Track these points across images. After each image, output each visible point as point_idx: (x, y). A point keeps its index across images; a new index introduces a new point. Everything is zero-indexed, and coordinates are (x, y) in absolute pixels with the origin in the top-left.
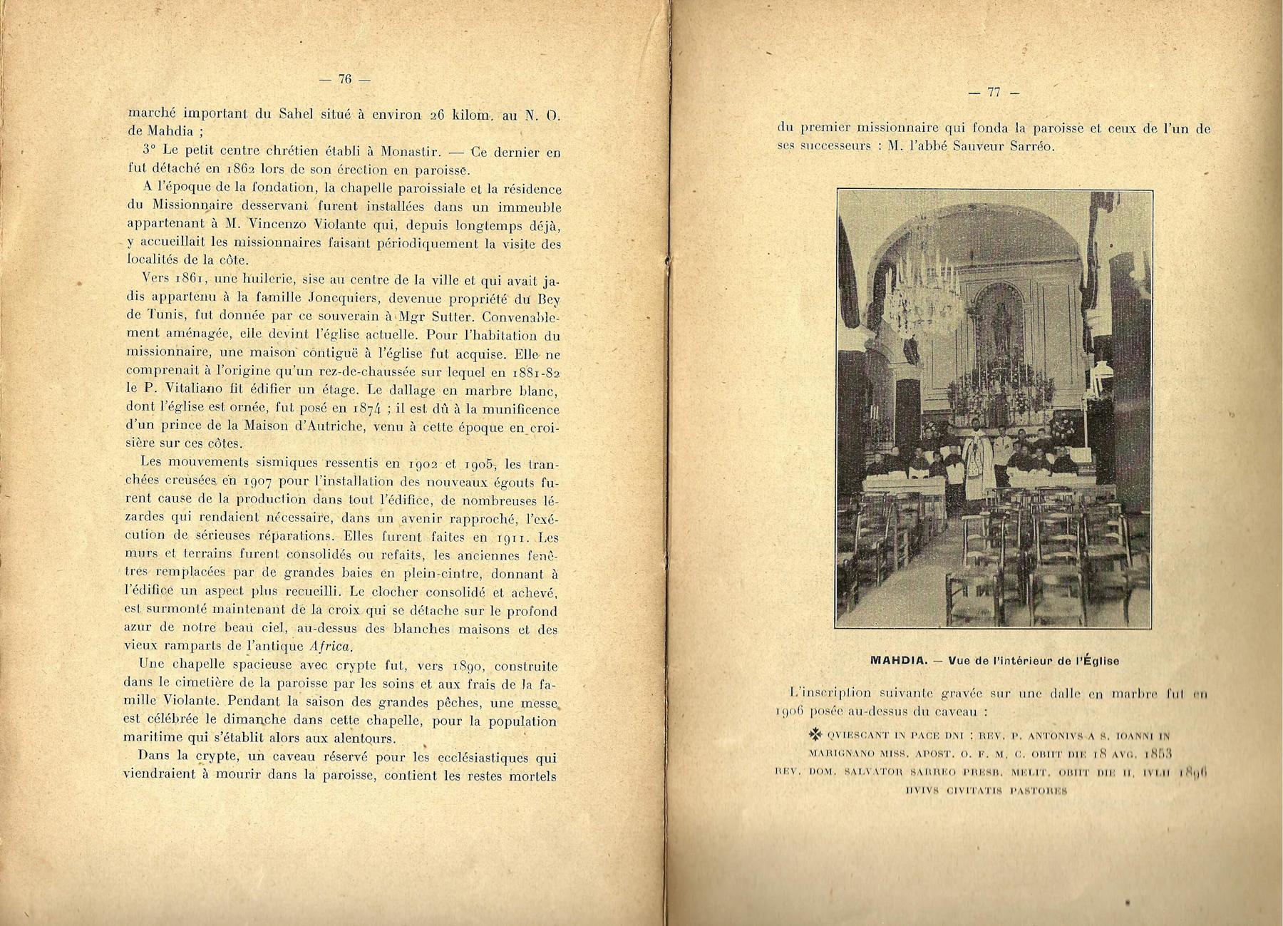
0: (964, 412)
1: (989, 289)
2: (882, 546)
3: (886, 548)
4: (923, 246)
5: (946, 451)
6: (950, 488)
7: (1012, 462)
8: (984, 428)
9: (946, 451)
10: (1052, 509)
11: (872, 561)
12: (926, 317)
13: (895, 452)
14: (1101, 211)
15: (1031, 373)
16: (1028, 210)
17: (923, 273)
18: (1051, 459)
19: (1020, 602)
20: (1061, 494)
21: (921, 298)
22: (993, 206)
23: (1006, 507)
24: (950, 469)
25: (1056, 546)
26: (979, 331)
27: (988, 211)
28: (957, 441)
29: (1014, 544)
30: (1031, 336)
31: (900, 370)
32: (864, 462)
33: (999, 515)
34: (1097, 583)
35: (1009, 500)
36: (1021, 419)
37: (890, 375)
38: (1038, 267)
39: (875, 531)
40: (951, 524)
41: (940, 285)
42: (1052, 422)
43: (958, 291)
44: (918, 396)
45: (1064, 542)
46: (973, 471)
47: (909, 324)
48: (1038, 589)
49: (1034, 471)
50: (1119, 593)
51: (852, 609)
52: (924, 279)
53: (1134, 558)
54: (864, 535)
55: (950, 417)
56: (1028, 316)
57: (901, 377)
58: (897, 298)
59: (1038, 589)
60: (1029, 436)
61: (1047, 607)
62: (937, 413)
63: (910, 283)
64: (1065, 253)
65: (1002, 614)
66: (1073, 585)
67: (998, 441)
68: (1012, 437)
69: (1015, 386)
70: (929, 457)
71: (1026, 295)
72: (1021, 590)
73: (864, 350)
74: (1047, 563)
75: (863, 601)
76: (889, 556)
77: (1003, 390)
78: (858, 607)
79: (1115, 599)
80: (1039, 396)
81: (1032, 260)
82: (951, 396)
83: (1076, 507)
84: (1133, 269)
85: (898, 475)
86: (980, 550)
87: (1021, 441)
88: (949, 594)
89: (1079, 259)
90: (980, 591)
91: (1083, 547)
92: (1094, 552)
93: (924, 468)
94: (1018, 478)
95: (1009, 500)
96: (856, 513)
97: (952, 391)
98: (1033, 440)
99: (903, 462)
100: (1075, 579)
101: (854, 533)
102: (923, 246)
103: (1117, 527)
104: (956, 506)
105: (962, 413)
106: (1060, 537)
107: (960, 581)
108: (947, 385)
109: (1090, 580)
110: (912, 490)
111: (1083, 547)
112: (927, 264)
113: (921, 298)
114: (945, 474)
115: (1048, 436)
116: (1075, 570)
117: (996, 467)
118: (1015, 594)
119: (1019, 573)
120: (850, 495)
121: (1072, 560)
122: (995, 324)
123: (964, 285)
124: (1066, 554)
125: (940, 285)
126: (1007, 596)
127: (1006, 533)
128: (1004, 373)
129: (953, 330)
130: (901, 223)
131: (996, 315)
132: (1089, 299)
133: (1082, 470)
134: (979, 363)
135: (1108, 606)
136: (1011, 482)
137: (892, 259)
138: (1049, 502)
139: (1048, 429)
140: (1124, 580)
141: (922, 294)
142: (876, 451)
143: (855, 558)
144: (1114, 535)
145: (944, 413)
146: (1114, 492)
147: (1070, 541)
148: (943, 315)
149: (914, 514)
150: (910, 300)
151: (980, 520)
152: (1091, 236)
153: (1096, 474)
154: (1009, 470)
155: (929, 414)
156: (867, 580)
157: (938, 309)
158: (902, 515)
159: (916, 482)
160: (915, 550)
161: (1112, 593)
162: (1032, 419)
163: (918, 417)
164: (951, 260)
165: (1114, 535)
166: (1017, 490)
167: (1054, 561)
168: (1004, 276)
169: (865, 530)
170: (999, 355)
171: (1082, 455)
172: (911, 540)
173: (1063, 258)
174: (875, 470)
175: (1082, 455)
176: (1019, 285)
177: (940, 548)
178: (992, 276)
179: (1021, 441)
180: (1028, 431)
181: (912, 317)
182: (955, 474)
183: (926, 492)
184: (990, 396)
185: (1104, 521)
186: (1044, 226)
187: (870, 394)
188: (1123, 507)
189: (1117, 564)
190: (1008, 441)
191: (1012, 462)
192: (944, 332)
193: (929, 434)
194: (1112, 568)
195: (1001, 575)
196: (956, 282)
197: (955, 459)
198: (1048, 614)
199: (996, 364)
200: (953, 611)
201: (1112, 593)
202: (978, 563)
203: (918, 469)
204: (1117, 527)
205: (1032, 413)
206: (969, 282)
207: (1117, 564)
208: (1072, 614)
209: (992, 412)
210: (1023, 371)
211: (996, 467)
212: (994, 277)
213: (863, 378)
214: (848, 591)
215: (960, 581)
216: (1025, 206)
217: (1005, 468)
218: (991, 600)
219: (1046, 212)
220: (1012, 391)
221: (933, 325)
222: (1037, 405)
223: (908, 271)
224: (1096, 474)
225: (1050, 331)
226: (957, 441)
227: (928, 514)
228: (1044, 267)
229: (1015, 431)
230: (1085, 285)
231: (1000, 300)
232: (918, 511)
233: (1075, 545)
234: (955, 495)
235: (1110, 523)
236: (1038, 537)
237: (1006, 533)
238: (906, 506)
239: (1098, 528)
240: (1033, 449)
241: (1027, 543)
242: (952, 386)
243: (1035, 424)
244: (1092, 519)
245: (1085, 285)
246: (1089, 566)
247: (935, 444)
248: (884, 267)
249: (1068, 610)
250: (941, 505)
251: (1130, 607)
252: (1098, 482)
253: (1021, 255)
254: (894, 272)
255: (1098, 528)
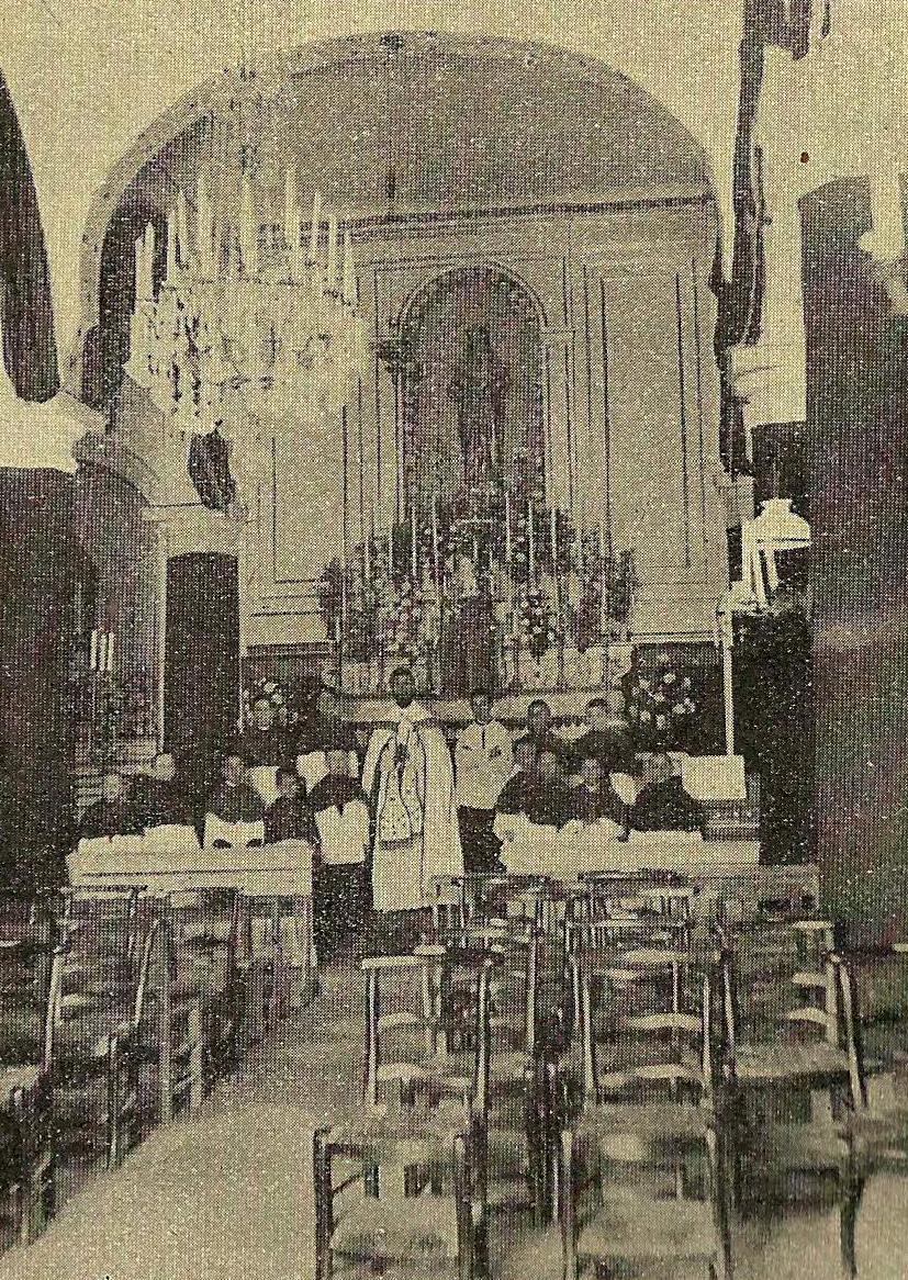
0: (367, 650)
1: (443, 287)
2: (124, 1046)
3: (135, 1053)
4: (246, 159)
5: (313, 767)
6: (328, 877)
7: (511, 799)
8: (426, 696)
9: (313, 767)
10: (629, 938)
11: (95, 1090)
12: (254, 370)
13: (165, 768)
14: (774, 54)
15: (565, 535)
16: (557, 53)
17: (247, 238)
18: (625, 788)
19: (536, 1213)
20: (656, 895)
21: (239, 311)
22: (453, 40)
23: (492, 931)
24: (326, 819)
25: (642, 1049)
26: (413, 411)
27: (439, 53)
28: (348, 737)
29: (517, 1041)
30: (567, 428)
31: (179, 523)
32: (70, 798)
33: (470, 956)
34: (763, 1155)
35: (501, 911)
36: (536, 671)
37: (148, 541)
38: (588, 220)
39: (104, 1003)
40: (330, 981)
41: (298, 273)
42: (628, 681)
43: (349, 291)
44: (233, 603)
45: (665, 1034)
46: (393, 825)
47: (205, 390)
48: (588, 1176)
49: (574, 824)
50: (829, 1187)
51: (35, 1235)
52: (250, 257)
53: (873, 1084)
54: (72, 1014)
55: (328, 665)
56: (557, 366)
57: (181, 548)
58: (168, 312)
59: (588, 1176)
60: (559, 721)
61: (615, 1228)
62: (291, 653)
63: (209, 268)
64: (668, 179)
65: (482, 1249)
66: (692, 1162)
67: (469, 736)
68: (510, 724)
69: (520, 574)
70: (265, 781)
71: (552, 304)
72: (538, 1177)
73: (70, 466)
74: (613, 1099)
75: (68, 1210)
76: (145, 1075)
77: (483, 585)
78: (53, 1228)
79: (815, 1204)
80: (590, 603)
81: (570, 198)
82: (329, 601)
83: (700, 933)
84: (867, 226)
85: (170, 837)
86: (415, 1058)
87: (536, 736)
88: (325, 1190)
89: (708, 197)
90: (415, 1180)
91: (720, 1050)
92: (753, 1065)
93: (250, 817)
94: (528, 845)
95: (501, 911)
96: (47, 949)
97: (333, 589)
98: (570, 734)
99: (186, 800)
100: (694, 1145)
101: (42, 1008)
102: (246, 159)
103: (820, 992)
104: (344, 930)
105: (363, 654)
106: (652, 1022)
107: (354, 1152)
108: (316, 571)
109: (742, 1147)
110: (214, 882)
111: (720, 1050)
112: (258, 211)
113: (239, 311)
114: (311, 834)
115: (617, 723)
116: (698, 1119)
117: (462, 811)
118: (520, 1190)
119: (532, 1127)
120: (29, 897)
121: (689, 1089)
122: (460, 389)
123: (368, 275)
124: (671, 1072)
125: (298, 273)
126: (494, 1197)
127: (491, 1010)
128: (486, 535)
129: (335, 408)
130: (179, 90)
131: (464, 363)
132: (738, 313)
133: (717, 823)
134: (412, 504)
135: (794, 1225)
136: (507, 857)
137: (154, 195)
138: (621, 918)
139: (616, 699)
140: (843, 1149)
141: (243, 300)
142: (107, 765)
143: (45, 1083)
144: (811, 1014)
145: (308, 653)
146: (813, 888)
147: (682, 1032)
148: (306, 363)
149: (221, 954)
150: (208, 318)
151: (414, 971)
152: (744, 128)
153: (759, 834)
154: (502, 823)
155: (265, 655)
156: (81, 1148)
157: (290, 346)
158: (183, 954)
159: (225, 859)
160: (223, 1059)
161: (807, 1187)
162: (570, 670)
163: (232, 665)
164: (331, 199)
165: (811, 1014)
166: (523, 882)
167: (635, 1093)
168: (488, 246)
169: (73, 1000)
170: (471, 480)
171: (716, 777)
172: (211, 1029)
173: (661, 193)
174: (104, 822)
175: (716, 777)
176: (530, 274)
177: (297, 1053)
178: (450, 246)
179: (536, 736)
180: (556, 705)
181: (214, 369)
182: (341, 834)
183: (253, 887)
184: (446, 603)
185: (784, 972)
186: (606, 98)
187: (90, 595)
188: (840, 933)
189: (821, 1101)
190: (499, 736)
191: (511, 799)
192: (310, 415)
193: (264, 715)
194: (806, 1114)
195: (478, 1132)
196: (344, 264)
197: (340, 789)
198: (616, 1249)
199: (462, 509)
200: (336, 1240)
201: (807, 1187)
202: (408, 1097)
203: (231, 818)
204: (820, 992)
205: (570, 652)
206: (383, 266)
207: (821, 1101)
208: (690, 1248)
209: (450, 649)
210: (541, 528)
211: (462, 811)
212: (458, 251)
213: (69, 551)
214: (25, 1182)
215: (354, 1152)
216: (551, 39)
217: (488, 816)
218: (448, 1205)
219: (609, 56)
220: (509, 588)
221: (275, 393)
222: (585, 629)
223: (203, 233)
224: (759, 834)
225: (622, 410)
226: (348, 737)
227: (262, 952)
228: (605, 220)
229: (519, 706)
230: (728, 275)
231: (474, 318)
232: (231, 944)
233: (697, 1045)
234: (341, 900)
235: (800, 979)
236: (586, 1020)
237: (491, 1010)
238: (195, 929)
239: (765, 994)
240: (571, 758)
241: (553, 1039)
242: (332, 573)
243: (578, 685)
244: (746, 968)
245: (728, 275)
246: (738, 1107)
247: (283, 746)
248: (130, 221)
249: (677, 1237)
250: (297, 925)
251: (861, 1227)
252: (767, 858)
253: (537, 187)
254: (161, 236)
255: (765, 994)
